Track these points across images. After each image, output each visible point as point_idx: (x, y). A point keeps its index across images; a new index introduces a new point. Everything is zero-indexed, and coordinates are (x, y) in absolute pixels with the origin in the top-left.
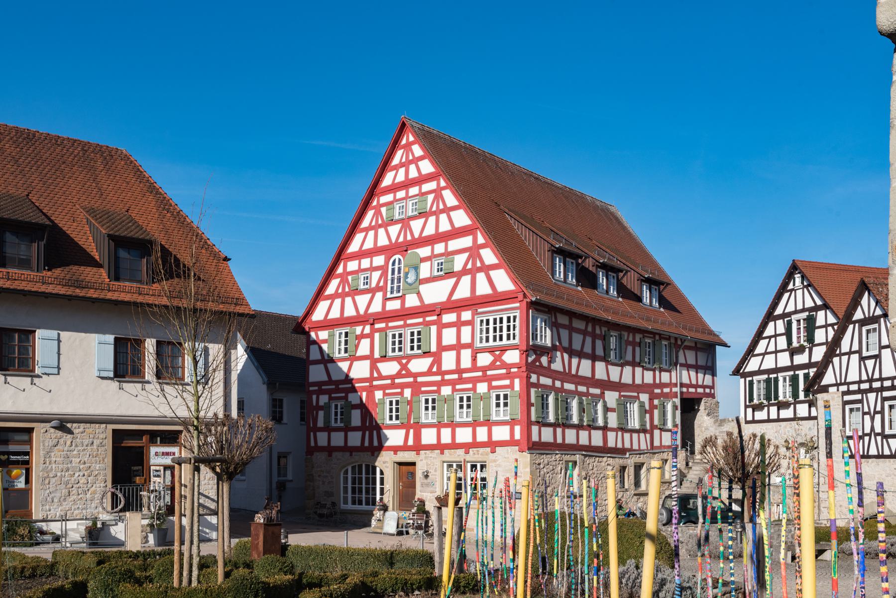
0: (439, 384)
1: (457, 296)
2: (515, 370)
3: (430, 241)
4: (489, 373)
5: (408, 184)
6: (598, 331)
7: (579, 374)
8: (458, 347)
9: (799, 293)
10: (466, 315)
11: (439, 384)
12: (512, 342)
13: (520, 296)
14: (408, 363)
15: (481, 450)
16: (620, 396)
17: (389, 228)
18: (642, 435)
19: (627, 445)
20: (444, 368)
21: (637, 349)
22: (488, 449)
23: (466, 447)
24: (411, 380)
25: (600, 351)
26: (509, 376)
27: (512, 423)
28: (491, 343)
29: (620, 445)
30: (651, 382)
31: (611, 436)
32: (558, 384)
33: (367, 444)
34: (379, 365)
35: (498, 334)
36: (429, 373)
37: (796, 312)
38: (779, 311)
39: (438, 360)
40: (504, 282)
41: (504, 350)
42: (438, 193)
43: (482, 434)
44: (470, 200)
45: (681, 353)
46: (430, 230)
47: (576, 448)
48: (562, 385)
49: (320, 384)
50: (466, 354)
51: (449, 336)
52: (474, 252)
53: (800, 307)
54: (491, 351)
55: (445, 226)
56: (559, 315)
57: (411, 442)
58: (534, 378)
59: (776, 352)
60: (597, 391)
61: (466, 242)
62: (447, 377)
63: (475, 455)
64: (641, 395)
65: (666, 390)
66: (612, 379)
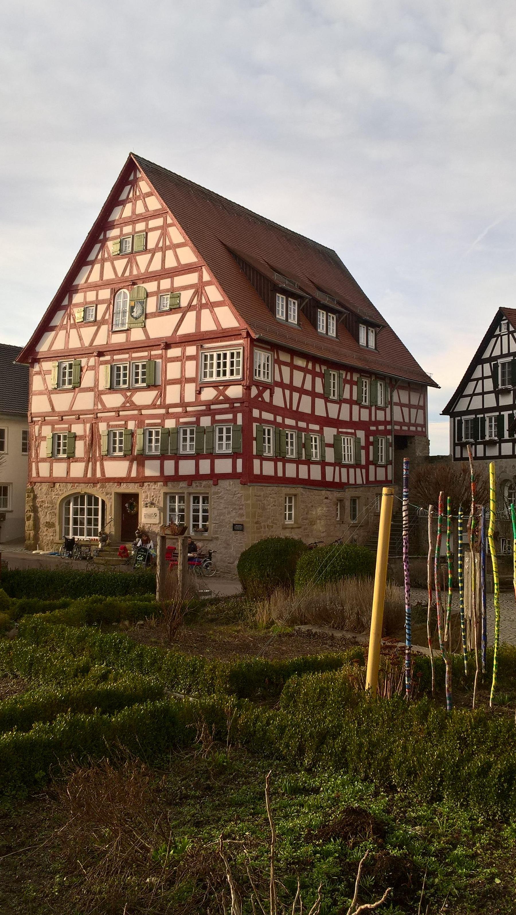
0: (163, 417)
1: (182, 331)
2: (238, 405)
3: (157, 276)
4: (213, 407)
5: (133, 221)
6: (318, 369)
7: (300, 410)
8: (182, 381)
9: (505, 338)
10: (191, 350)
11: (163, 417)
12: (235, 377)
13: (244, 334)
14: (131, 396)
15: (204, 483)
16: (339, 432)
17: (116, 262)
18: (358, 470)
19: (344, 480)
20: (168, 401)
21: (355, 388)
22: (211, 482)
23: (190, 479)
24: (136, 412)
25: (319, 389)
26: (232, 410)
27: (234, 456)
28: (215, 378)
29: (337, 480)
30: (367, 419)
31: (329, 470)
32: (279, 419)
33: (89, 475)
34: (104, 397)
35: (221, 369)
36: (153, 406)
37: (502, 356)
38: (486, 355)
39: (162, 395)
40: (228, 318)
41: (227, 384)
42: (164, 228)
43: (205, 466)
44: (196, 237)
46: (156, 266)
47: (296, 481)
48: (283, 421)
49: (43, 416)
50: (190, 389)
51: (173, 371)
52: (199, 289)
53: (505, 351)
54: (215, 385)
55: (171, 263)
56: (280, 353)
57: (134, 474)
58: (256, 413)
59: (483, 393)
60: (317, 427)
61: (192, 278)
62: (171, 410)
63: (198, 488)
64: (357, 431)
65: (381, 428)
66: (330, 416)
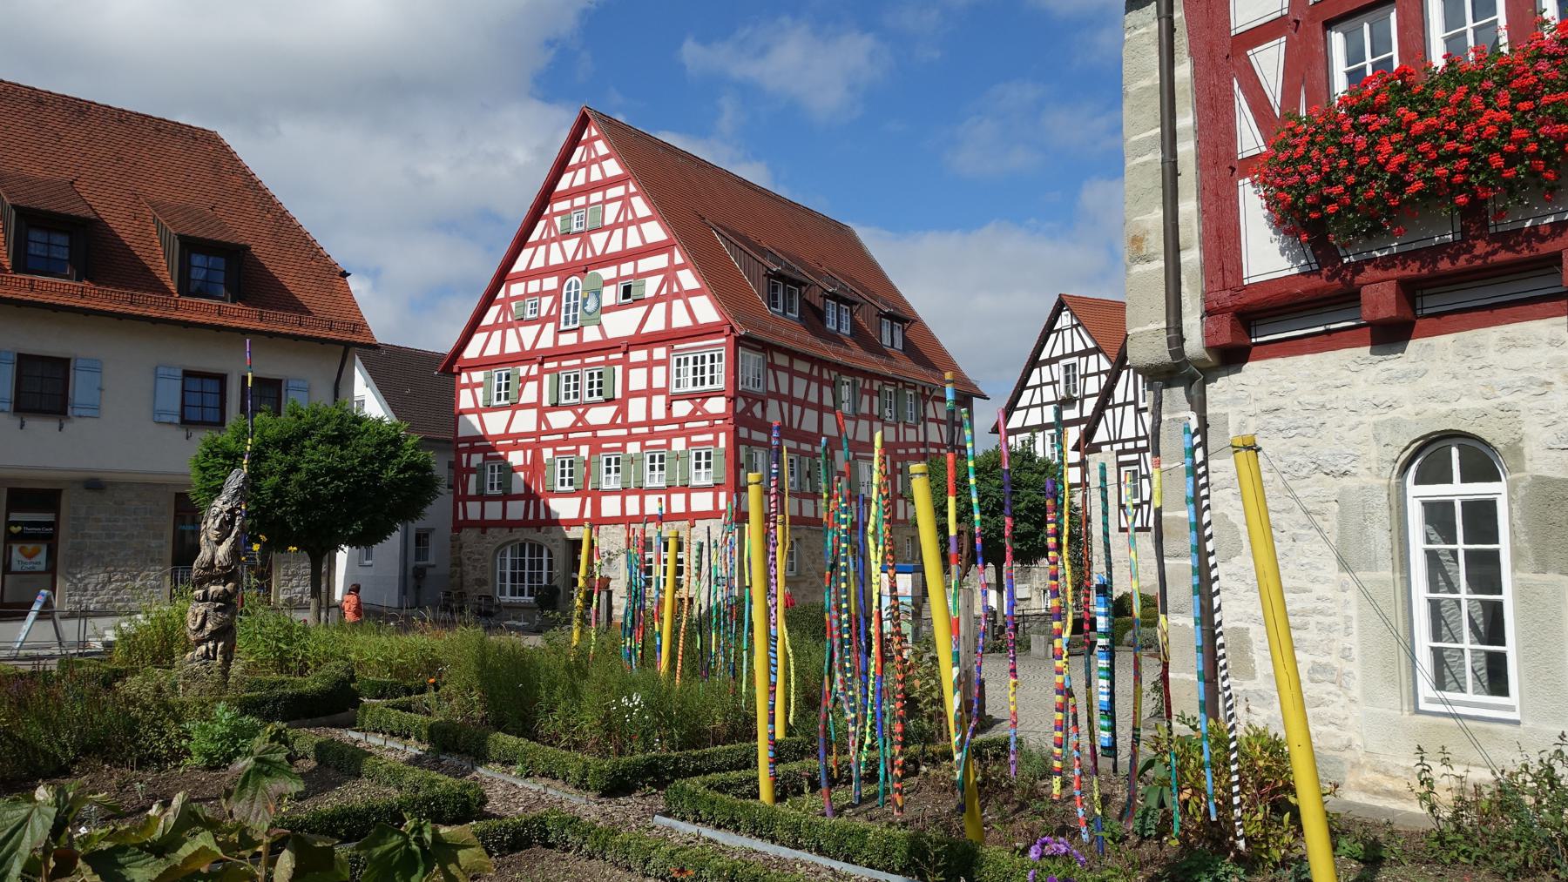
5: (587, 190)
6: (826, 376)
8: (649, 393)
9: (1067, 333)
10: (660, 353)
12: (716, 386)
13: (727, 330)
14: (585, 413)
16: (855, 458)
20: (631, 419)
21: (876, 399)
24: (589, 434)
25: (828, 401)
26: (712, 429)
27: (716, 488)
28: (690, 388)
33: (531, 517)
34: (549, 415)
36: (612, 425)
37: (1064, 356)
38: (1044, 355)
39: (623, 410)
40: (706, 311)
41: (706, 396)
42: (625, 201)
44: (664, 209)
45: (930, 405)
46: (615, 246)
50: (659, 402)
51: (638, 379)
52: (669, 274)
53: (1068, 350)
54: (690, 397)
55: (634, 242)
58: (743, 432)
59: (1042, 405)
61: (661, 261)
62: (634, 431)
